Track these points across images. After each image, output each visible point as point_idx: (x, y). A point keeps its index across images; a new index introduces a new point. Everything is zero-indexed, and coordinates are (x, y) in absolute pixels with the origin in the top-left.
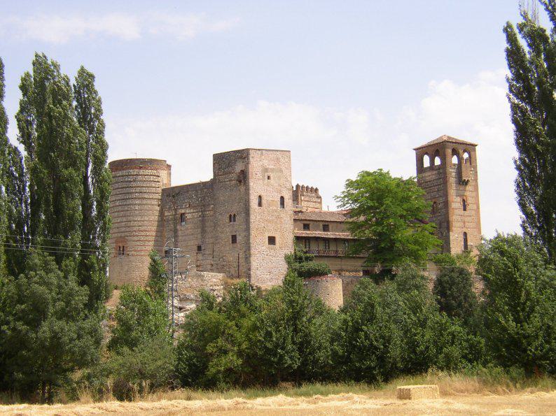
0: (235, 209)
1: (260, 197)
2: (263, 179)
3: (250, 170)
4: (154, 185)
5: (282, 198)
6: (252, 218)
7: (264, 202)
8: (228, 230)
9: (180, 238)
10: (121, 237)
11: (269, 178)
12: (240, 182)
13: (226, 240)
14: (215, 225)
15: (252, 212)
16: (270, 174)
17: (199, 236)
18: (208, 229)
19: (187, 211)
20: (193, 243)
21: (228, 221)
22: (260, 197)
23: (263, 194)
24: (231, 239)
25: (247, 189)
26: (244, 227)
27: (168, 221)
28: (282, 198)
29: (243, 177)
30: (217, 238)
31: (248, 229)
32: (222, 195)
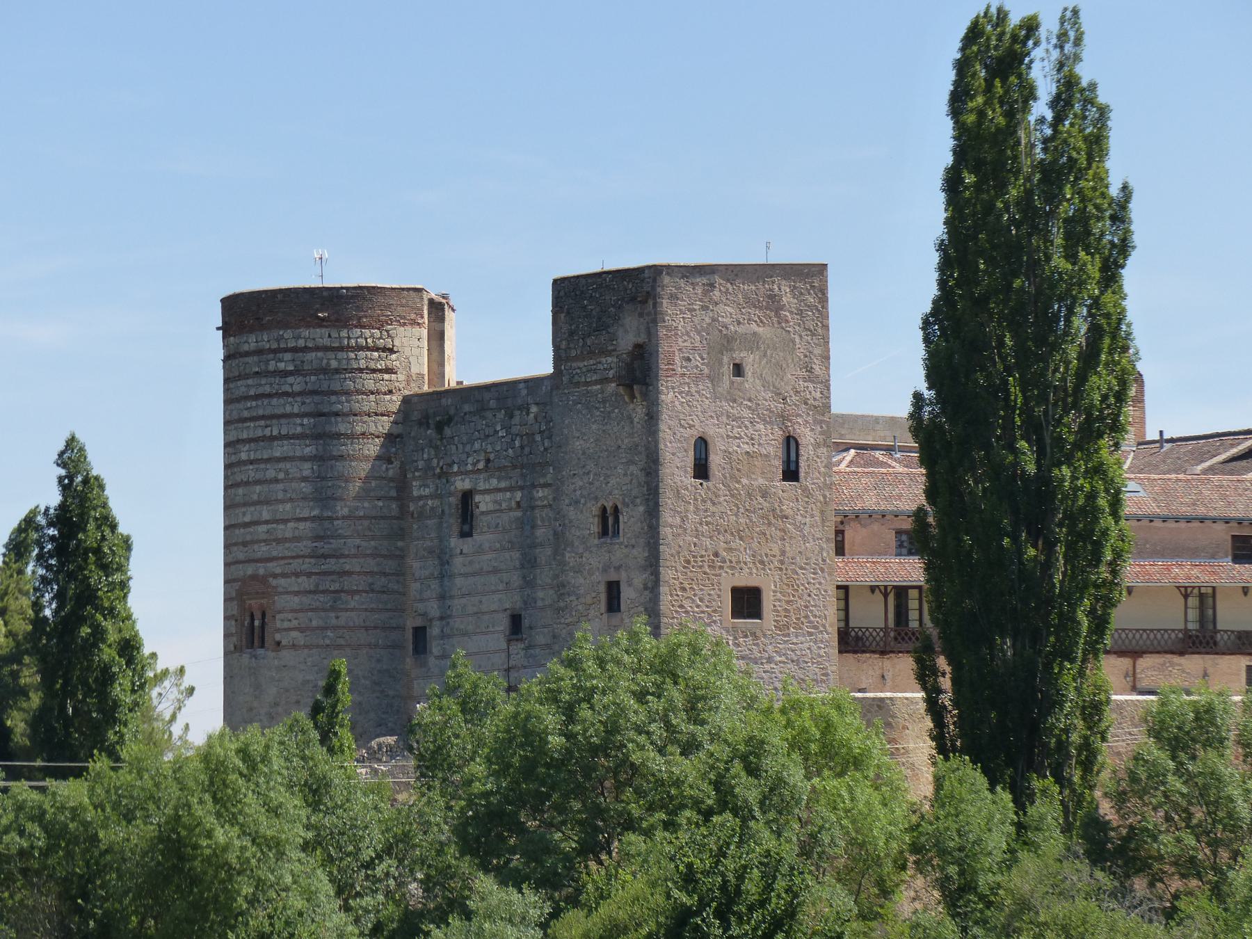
0: (618, 484)
1: (702, 444)
2: (714, 379)
3: (664, 347)
4: (370, 385)
5: (791, 443)
6: (668, 517)
7: (715, 460)
9: (459, 581)
10: (254, 577)
11: (738, 370)
12: (629, 387)
13: (589, 600)
14: (559, 540)
15: (667, 499)
16: (739, 356)
18: (544, 554)
19: (482, 486)
20: (498, 602)
21: (595, 528)
22: (702, 444)
23: (713, 431)
24: (603, 597)
25: (652, 418)
26: (640, 554)
27: (421, 515)
28: (791, 443)
29: (640, 373)
30: (561, 589)
31: (653, 564)
32: (583, 436)
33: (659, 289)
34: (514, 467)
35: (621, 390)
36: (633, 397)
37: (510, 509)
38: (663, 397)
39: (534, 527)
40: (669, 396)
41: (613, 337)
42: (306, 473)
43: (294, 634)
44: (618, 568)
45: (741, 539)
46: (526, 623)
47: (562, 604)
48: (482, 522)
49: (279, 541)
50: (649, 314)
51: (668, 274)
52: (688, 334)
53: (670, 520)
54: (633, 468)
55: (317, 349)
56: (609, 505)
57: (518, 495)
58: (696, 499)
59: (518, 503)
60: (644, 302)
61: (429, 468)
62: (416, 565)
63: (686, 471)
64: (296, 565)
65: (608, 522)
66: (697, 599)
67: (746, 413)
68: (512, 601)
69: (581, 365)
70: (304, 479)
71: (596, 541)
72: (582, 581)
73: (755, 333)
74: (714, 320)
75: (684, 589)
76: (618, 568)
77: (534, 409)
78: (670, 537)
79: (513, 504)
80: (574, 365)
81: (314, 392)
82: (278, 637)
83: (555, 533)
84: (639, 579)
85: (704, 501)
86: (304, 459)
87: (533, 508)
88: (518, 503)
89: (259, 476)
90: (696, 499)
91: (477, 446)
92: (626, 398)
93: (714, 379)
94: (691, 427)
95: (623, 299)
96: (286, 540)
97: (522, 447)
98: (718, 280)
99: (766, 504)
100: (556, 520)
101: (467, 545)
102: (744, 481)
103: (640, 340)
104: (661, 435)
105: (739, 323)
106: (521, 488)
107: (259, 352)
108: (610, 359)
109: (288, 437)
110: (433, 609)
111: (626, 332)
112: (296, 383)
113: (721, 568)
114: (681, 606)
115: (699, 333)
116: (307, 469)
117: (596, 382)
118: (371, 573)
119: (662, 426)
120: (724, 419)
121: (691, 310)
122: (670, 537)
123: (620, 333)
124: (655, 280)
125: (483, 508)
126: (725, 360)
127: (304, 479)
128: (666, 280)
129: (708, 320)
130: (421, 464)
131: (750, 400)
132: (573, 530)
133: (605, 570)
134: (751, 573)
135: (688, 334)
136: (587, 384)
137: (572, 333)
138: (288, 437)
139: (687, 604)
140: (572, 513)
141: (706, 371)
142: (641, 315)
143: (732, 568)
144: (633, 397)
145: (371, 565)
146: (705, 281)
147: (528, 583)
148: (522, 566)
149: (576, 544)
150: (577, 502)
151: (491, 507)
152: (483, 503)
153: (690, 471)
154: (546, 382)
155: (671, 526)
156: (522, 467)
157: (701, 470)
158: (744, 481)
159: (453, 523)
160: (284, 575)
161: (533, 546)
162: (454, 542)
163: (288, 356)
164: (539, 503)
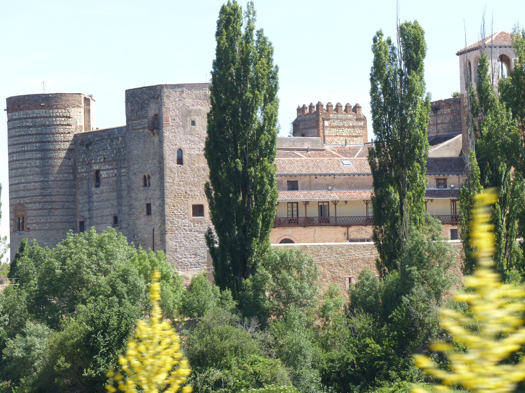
0: (149, 167)
1: (180, 152)
2: (184, 127)
3: (165, 115)
4: (61, 130)
6: (167, 179)
7: (185, 157)
8: (142, 196)
9: (95, 204)
10: (19, 204)
11: (193, 123)
12: (152, 130)
13: (140, 211)
14: (129, 188)
15: (167, 172)
16: (193, 118)
17: (115, 203)
19: (103, 168)
20: (109, 212)
21: (142, 183)
23: (184, 146)
24: (145, 209)
25: (161, 142)
26: (158, 193)
27: (82, 179)
29: (156, 125)
30: (130, 207)
31: (162, 197)
32: (137, 149)
33: (162, 94)
34: (114, 161)
35: (150, 132)
36: (154, 134)
37: (113, 177)
38: (165, 134)
39: (121, 183)
40: (167, 134)
41: (147, 112)
42: (38, 164)
43: (35, 225)
44: (150, 199)
45: (196, 186)
46: (119, 219)
47: (131, 212)
48: (103, 181)
49: (28, 190)
50: (159, 103)
51: (166, 88)
52: (174, 110)
53: (168, 180)
54: (155, 161)
55: (41, 117)
56: (146, 175)
57: (115, 171)
58: (178, 172)
59: (115, 174)
60: (157, 98)
61: (84, 161)
62: (80, 198)
63: (174, 162)
64: (35, 199)
65: (146, 181)
66: (179, 210)
67: (197, 139)
68: (113, 211)
69: (136, 122)
70: (37, 167)
71: (142, 189)
72: (138, 203)
73: (199, 109)
74: (184, 104)
75: (174, 206)
76: (150, 199)
77: (120, 139)
78: (168, 187)
79: (114, 175)
80: (133, 122)
81: (40, 134)
82: (28, 226)
83: (128, 186)
84: (158, 203)
85: (181, 173)
86: (37, 159)
87: (121, 176)
88: (115, 174)
89: (21, 166)
90: (178, 172)
91: (101, 153)
92: (152, 135)
93: (184, 127)
94: (176, 145)
95: (150, 97)
96: (31, 190)
97: (116, 153)
98: (185, 89)
99: (205, 173)
100: (128, 180)
101: (98, 190)
102: (196, 165)
103: (156, 113)
104: (164, 148)
105: (193, 105)
106: (117, 169)
107: (20, 119)
108: (146, 120)
109: (31, 151)
110: (86, 214)
111: (151, 110)
112: (33, 131)
113: (188, 198)
114: (173, 213)
115: (178, 110)
116: (38, 163)
117: (141, 129)
118: (63, 202)
119: (165, 145)
120: (188, 142)
121: (175, 101)
122: (168, 187)
123: (149, 110)
124: (161, 90)
125: (103, 176)
126: (188, 119)
127: (37, 167)
128: (165, 90)
129: (181, 105)
130: (81, 160)
131: (198, 134)
132: (134, 184)
133: (146, 199)
134: (199, 200)
135: (174, 110)
136: (138, 129)
137: (132, 110)
138: (31, 151)
139: (175, 212)
140: (134, 178)
141: (181, 124)
142: (156, 103)
143: (192, 198)
144: (154, 134)
145: (63, 198)
146: (180, 90)
147: (120, 204)
148: (117, 198)
149: (135, 189)
150: (135, 174)
151: (106, 176)
152: (103, 174)
153: (176, 161)
154: (124, 129)
155: (169, 183)
156: (117, 161)
157: (180, 161)
158: (196, 165)
159: (93, 182)
160: (30, 203)
161: (121, 190)
162: (93, 189)
163: (30, 120)
164: (123, 174)
